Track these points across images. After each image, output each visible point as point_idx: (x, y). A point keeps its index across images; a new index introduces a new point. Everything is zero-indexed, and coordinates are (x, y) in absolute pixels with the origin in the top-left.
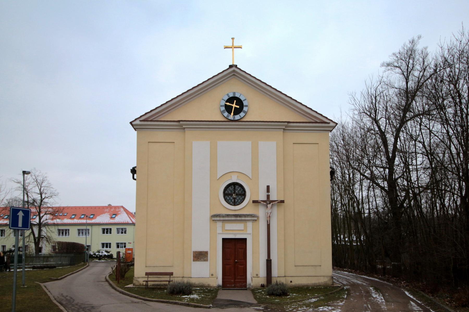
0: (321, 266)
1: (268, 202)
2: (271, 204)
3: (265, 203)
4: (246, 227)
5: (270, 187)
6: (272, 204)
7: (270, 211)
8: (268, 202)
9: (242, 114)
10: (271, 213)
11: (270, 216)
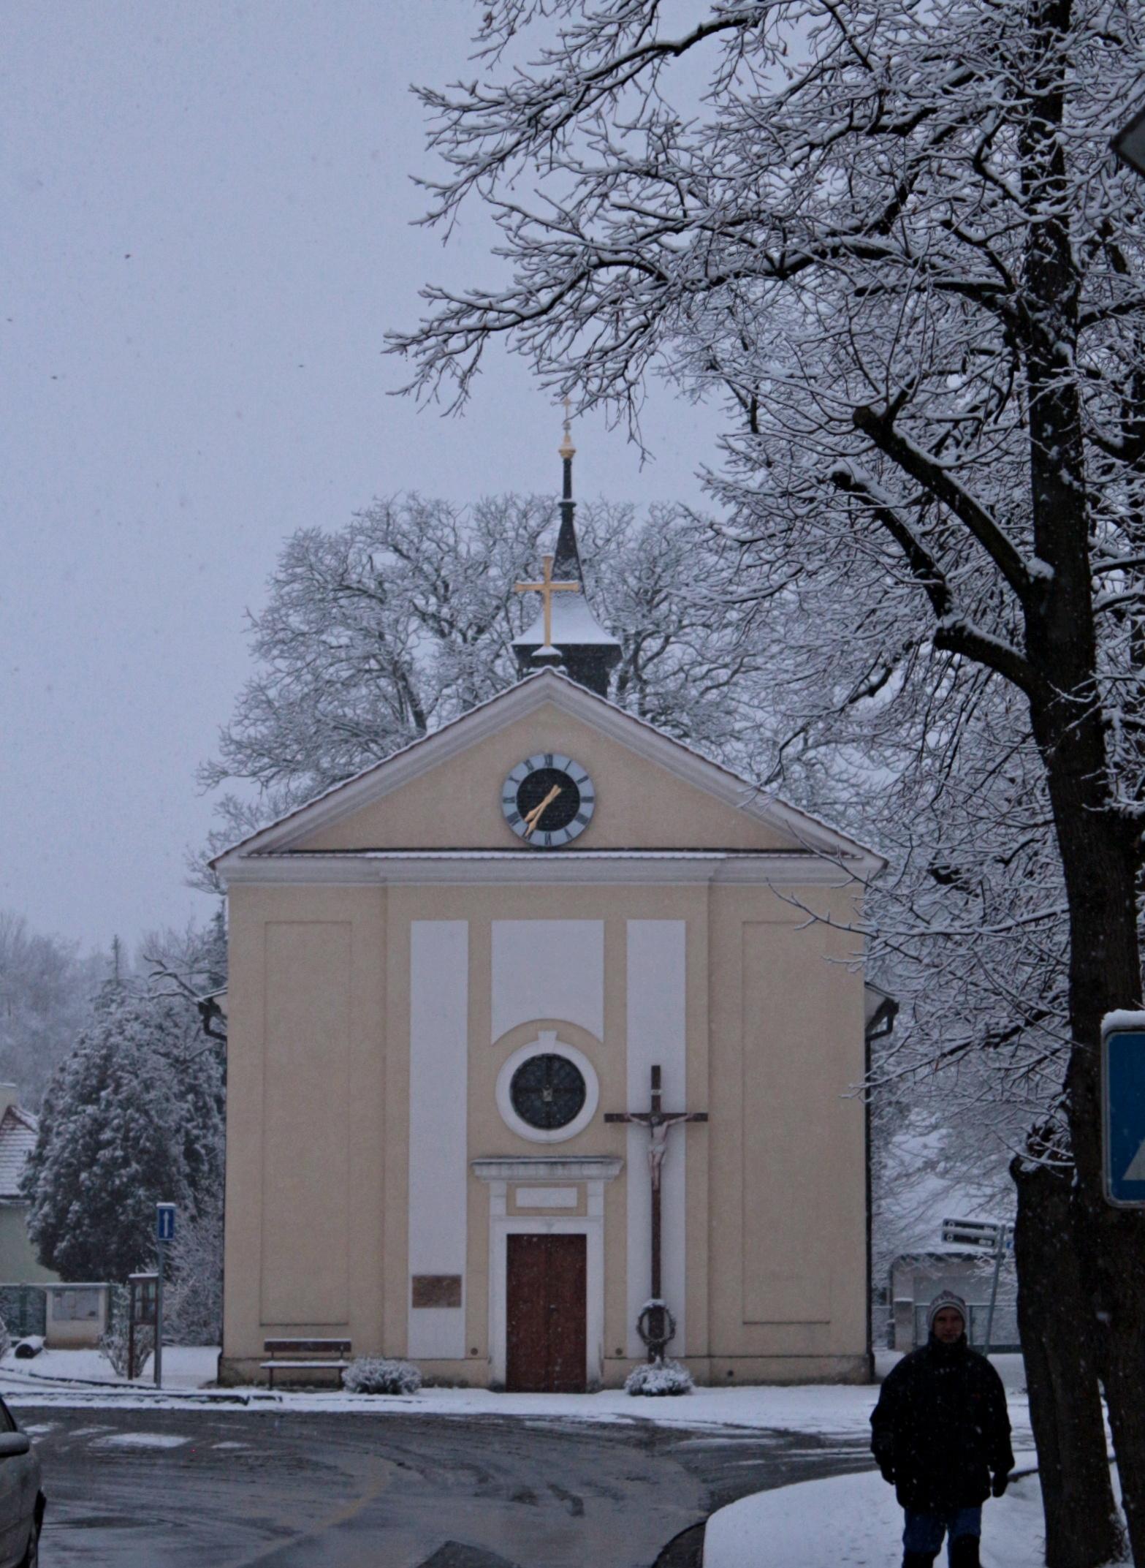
0: (828, 1323)
1: (655, 1120)
2: (665, 1124)
3: (644, 1123)
4: (583, 1197)
5: (663, 1069)
6: (669, 1126)
7: (660, 1148)
8: (656, 1116)
9: (575, 827)
10: (663, 1154)
11: (659, 1164)
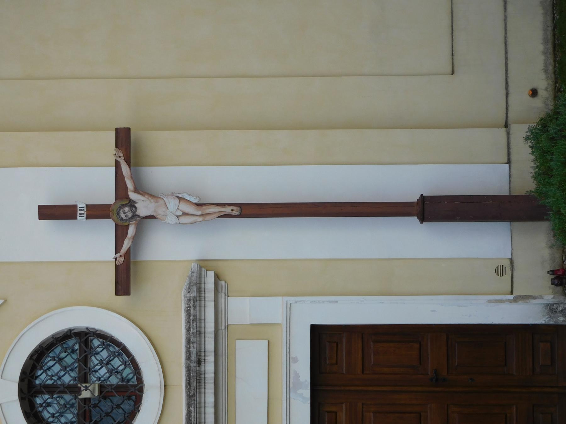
1: (126, 213)
2: (133, 196)
3: (131, 231)
6: (136, 191)
7: (172, 204)
10: (180, 199)
11: (198, 205)
